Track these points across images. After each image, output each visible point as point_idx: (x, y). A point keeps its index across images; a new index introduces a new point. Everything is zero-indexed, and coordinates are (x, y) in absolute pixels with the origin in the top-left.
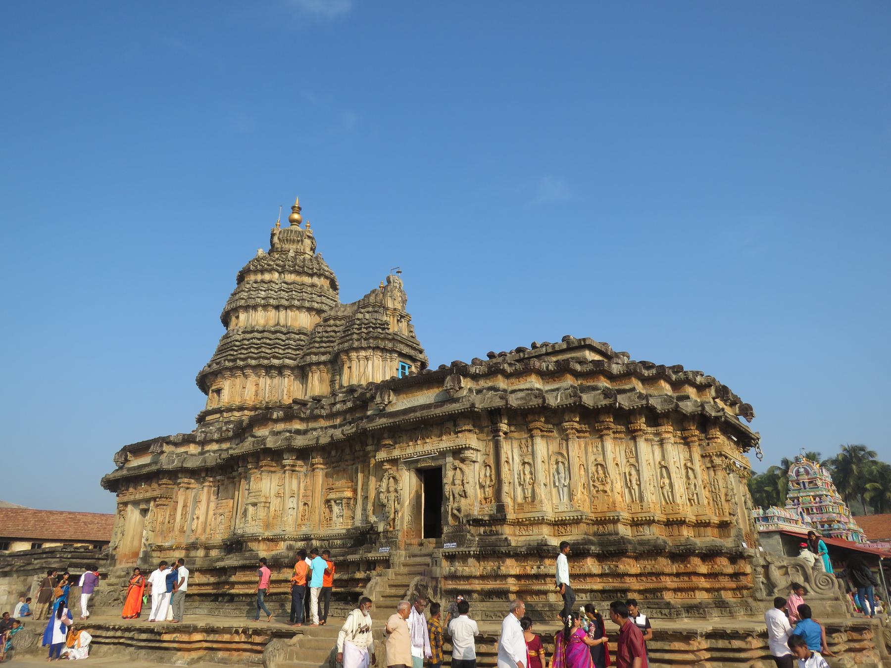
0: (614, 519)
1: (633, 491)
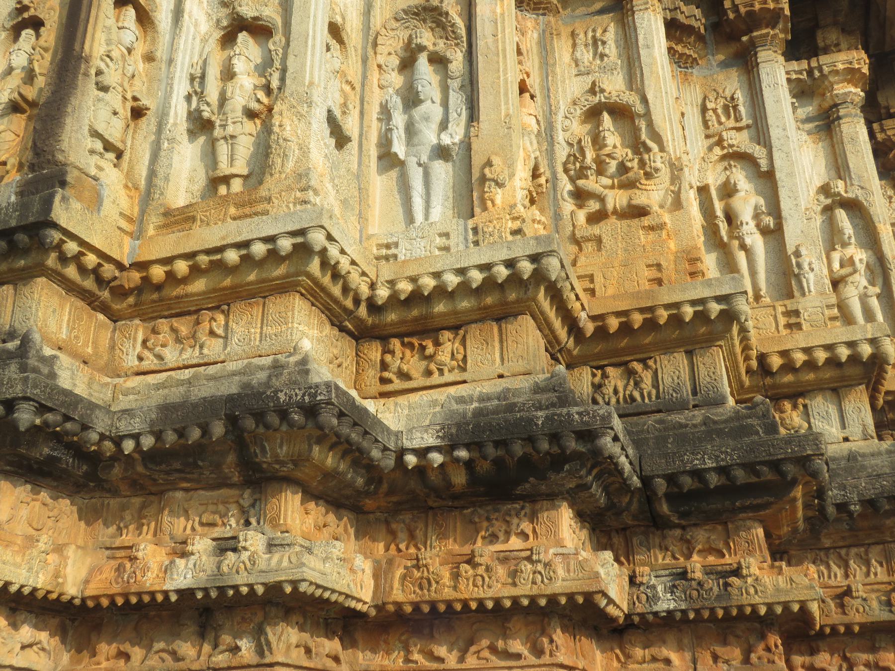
0: (701, 316)
1: (741, 258)
